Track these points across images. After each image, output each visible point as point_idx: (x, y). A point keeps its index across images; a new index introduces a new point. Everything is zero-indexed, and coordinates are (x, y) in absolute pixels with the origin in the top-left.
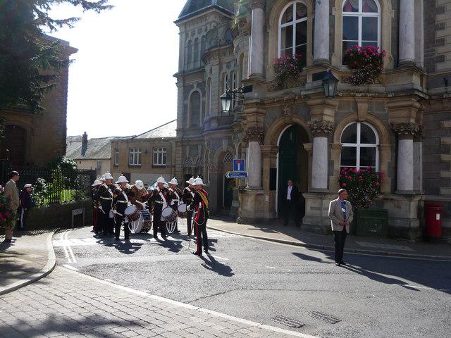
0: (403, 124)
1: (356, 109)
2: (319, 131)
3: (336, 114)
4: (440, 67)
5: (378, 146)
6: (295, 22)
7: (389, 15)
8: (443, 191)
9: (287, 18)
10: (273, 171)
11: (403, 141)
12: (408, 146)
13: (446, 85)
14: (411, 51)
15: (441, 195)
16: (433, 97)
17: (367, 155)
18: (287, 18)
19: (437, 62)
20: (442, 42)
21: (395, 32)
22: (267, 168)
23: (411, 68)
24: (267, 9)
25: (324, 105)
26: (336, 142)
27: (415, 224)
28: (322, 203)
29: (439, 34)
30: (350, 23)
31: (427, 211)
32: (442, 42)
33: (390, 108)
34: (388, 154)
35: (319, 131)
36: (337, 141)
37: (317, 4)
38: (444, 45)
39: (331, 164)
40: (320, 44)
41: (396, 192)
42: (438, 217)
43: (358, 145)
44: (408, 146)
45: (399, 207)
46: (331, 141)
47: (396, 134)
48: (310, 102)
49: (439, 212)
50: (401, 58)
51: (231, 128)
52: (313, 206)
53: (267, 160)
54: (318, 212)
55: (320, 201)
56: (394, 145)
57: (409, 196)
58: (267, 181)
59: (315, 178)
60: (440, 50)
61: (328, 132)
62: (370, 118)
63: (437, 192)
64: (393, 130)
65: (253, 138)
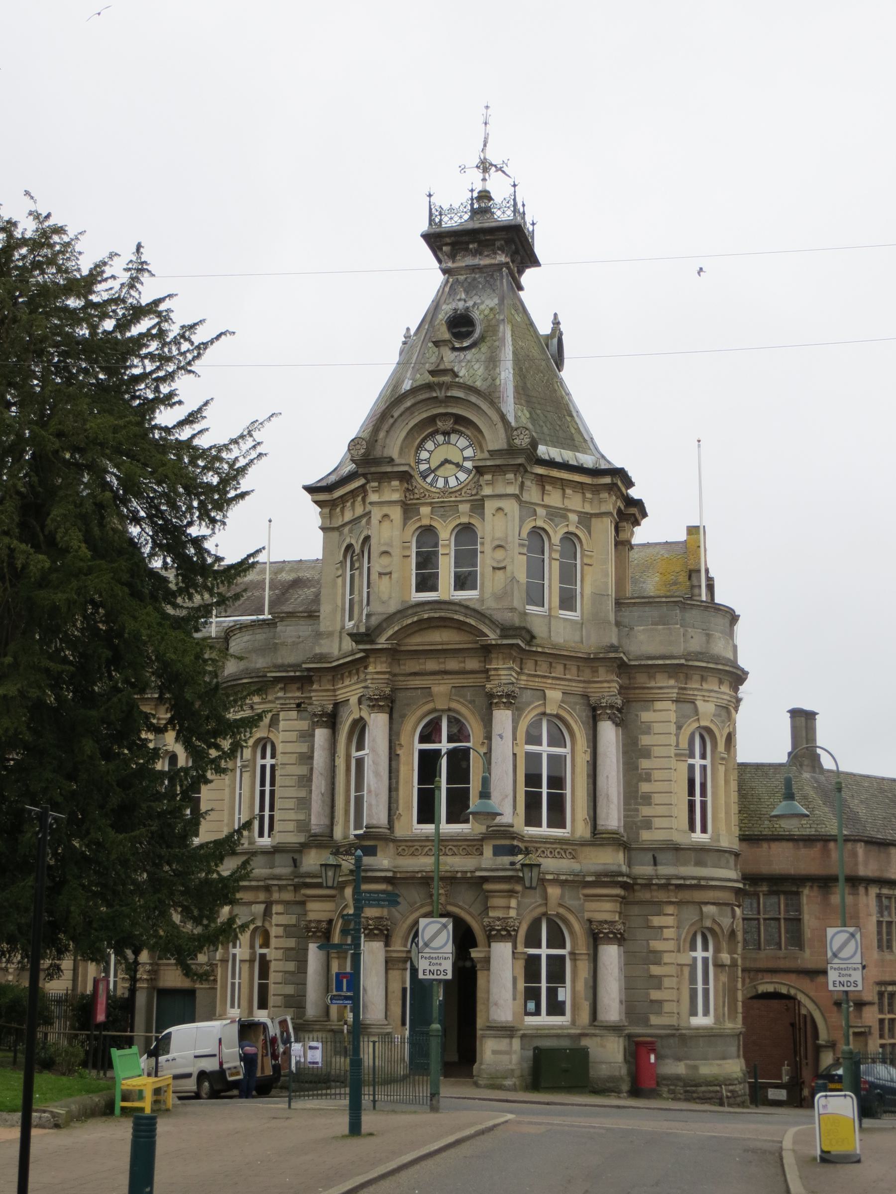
0: (606, 922)
1: (545, 897)
2: (504, 933)
3: (519, 904)
4: (645, 835)
5: (572, 954)
6: (444, 746)
7: (583, 758)
8: (654, 1020)
9: (430, 734)
10: (404, 990)
11: (605, 947)
12: (611, 954)
13: (655, 864)
14: (612, 818)
15: (651, 1026)
16: (639, 881)
17: (557, 963)
18: (430, 734)
19: (642, 828)
20: (647, 799)
21: (591, 786)
22: (396, 987)
23: (615, 841)
24: (395, 716)
25: (511, 893)
26: (521, 948)
27: (624, 1071)
28: (511, 1044)
29: (645, 787)
30: (533, 759)
31: (637, 1049)
32: (647, 799)
33: (586, 896)
34: (584, 968)
35: (504, 933)
36: (521, 948)
37: (495, 740)
38: (650, 804)
39: (515, 980)
40: (503, 799)
41: (596, 1023)
42: (652, 1058)
43: (544, 951)
44: (611, 954)
45: (603, 1046)
46: (515, 947)
47: (596, 937)
48: (488, 886)
49: (653, 1051)
50: (600, 822)
51: (303, 903)
52: (496, 1048)
53: (395, 974)
54: (505, 1058)
55: (507, 1041)
56: (592, 952)
57: (615, 1029)
58: (396, 1010)
59: (496, 1004)
60: (645, 811)
61: (507, 934)
62: (562, 911)
63: (646, 1022)
64: (592, 930)
65: (376, 935)
